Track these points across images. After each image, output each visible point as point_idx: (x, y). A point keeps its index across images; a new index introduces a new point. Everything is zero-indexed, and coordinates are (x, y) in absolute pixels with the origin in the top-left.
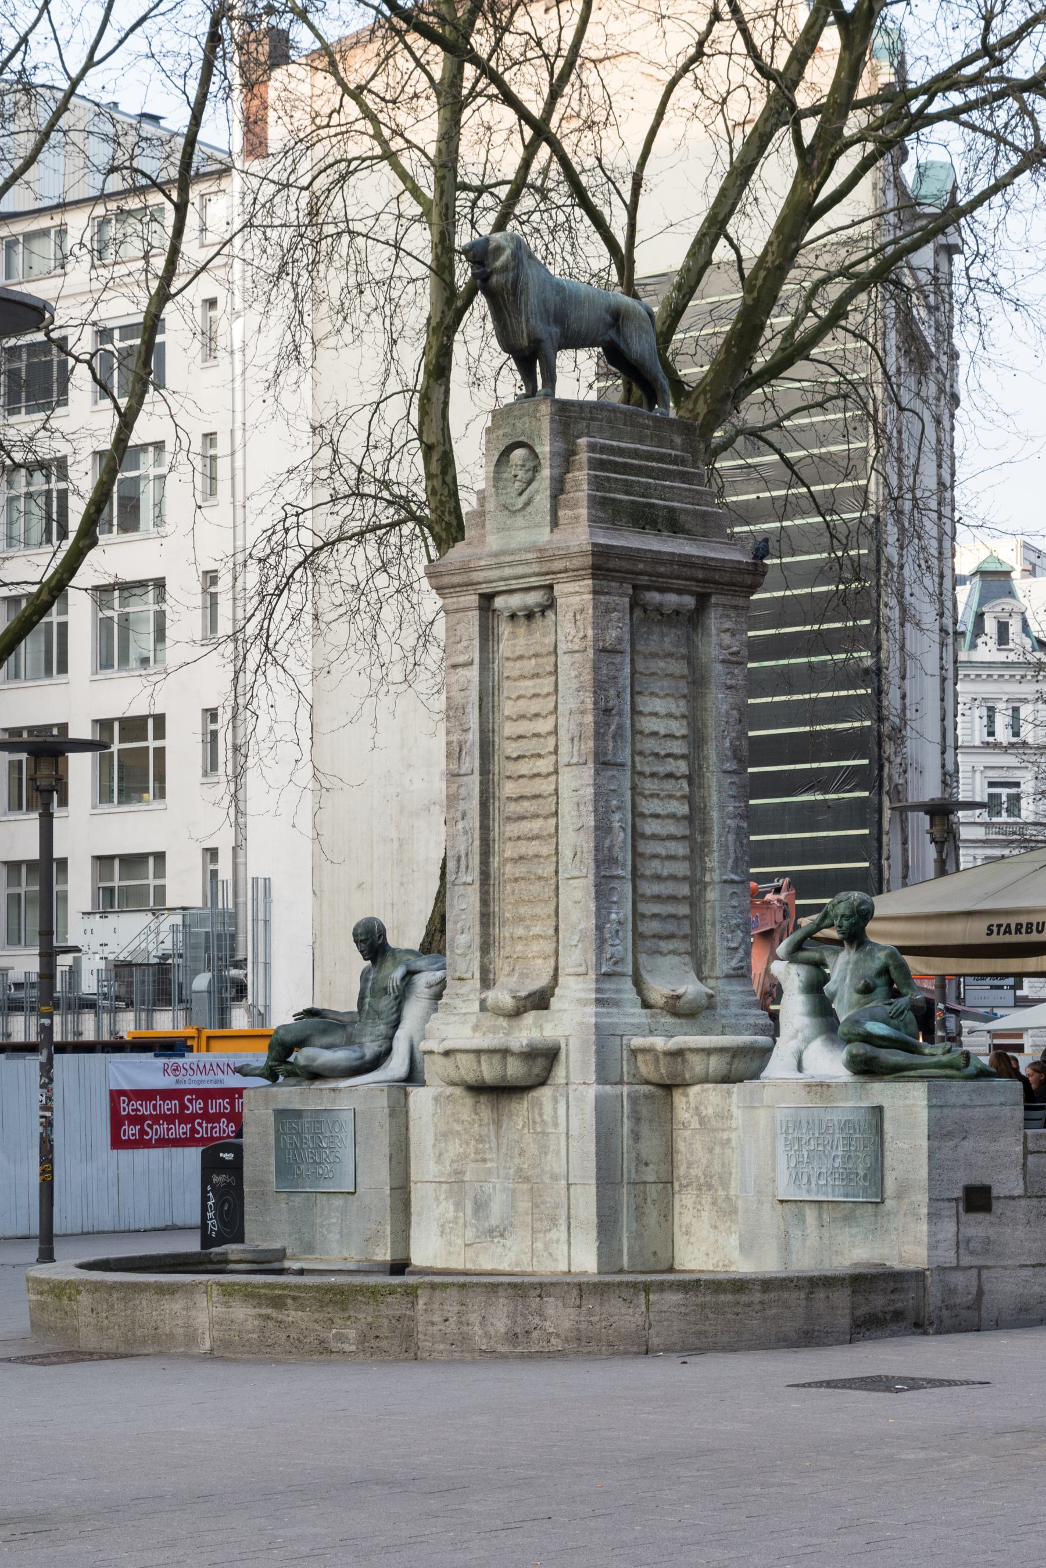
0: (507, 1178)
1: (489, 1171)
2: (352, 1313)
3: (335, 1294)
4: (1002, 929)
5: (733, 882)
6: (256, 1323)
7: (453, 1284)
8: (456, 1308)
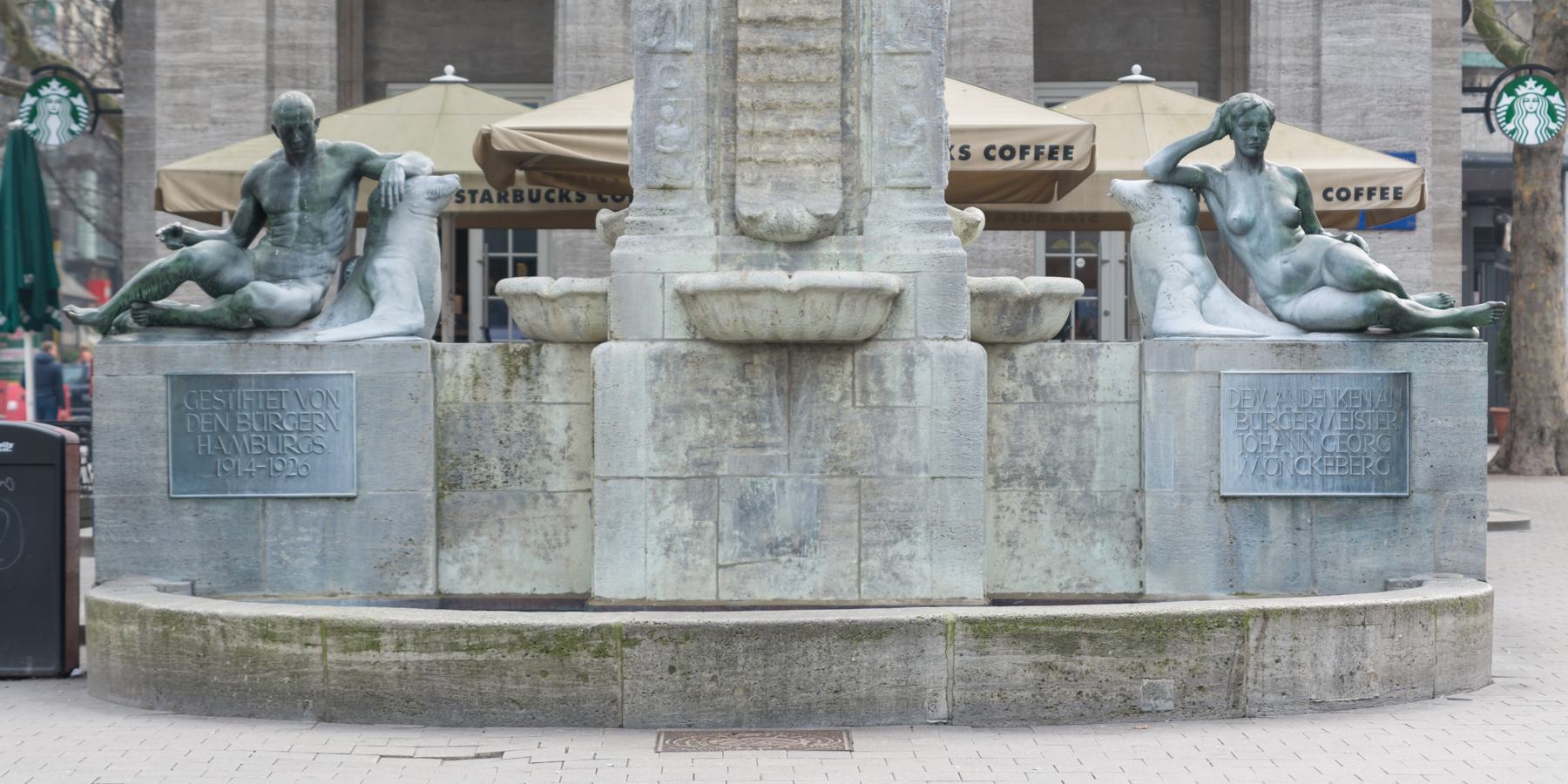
0: (808, 469)
1: (771, 462)
2: (1170, 656)
3: (1149, 630)
6: (1030, 675)
7: (1310, 610)
8: (1288, 644)
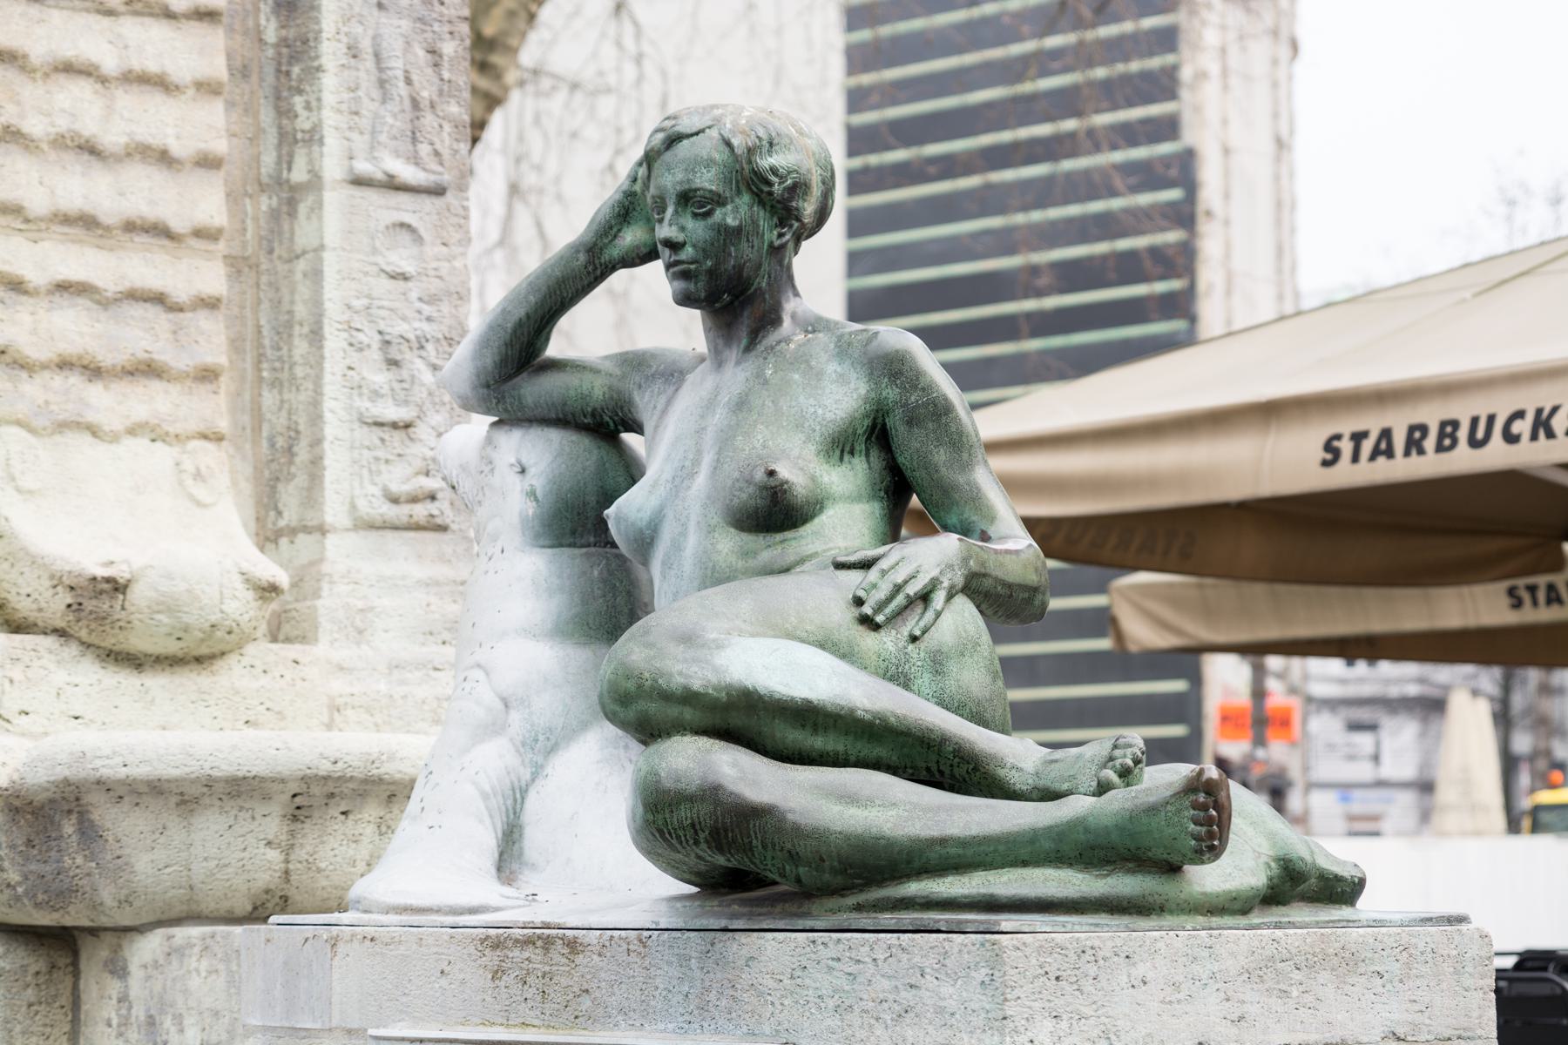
4: (1367, 446)
5: (393, 185)
